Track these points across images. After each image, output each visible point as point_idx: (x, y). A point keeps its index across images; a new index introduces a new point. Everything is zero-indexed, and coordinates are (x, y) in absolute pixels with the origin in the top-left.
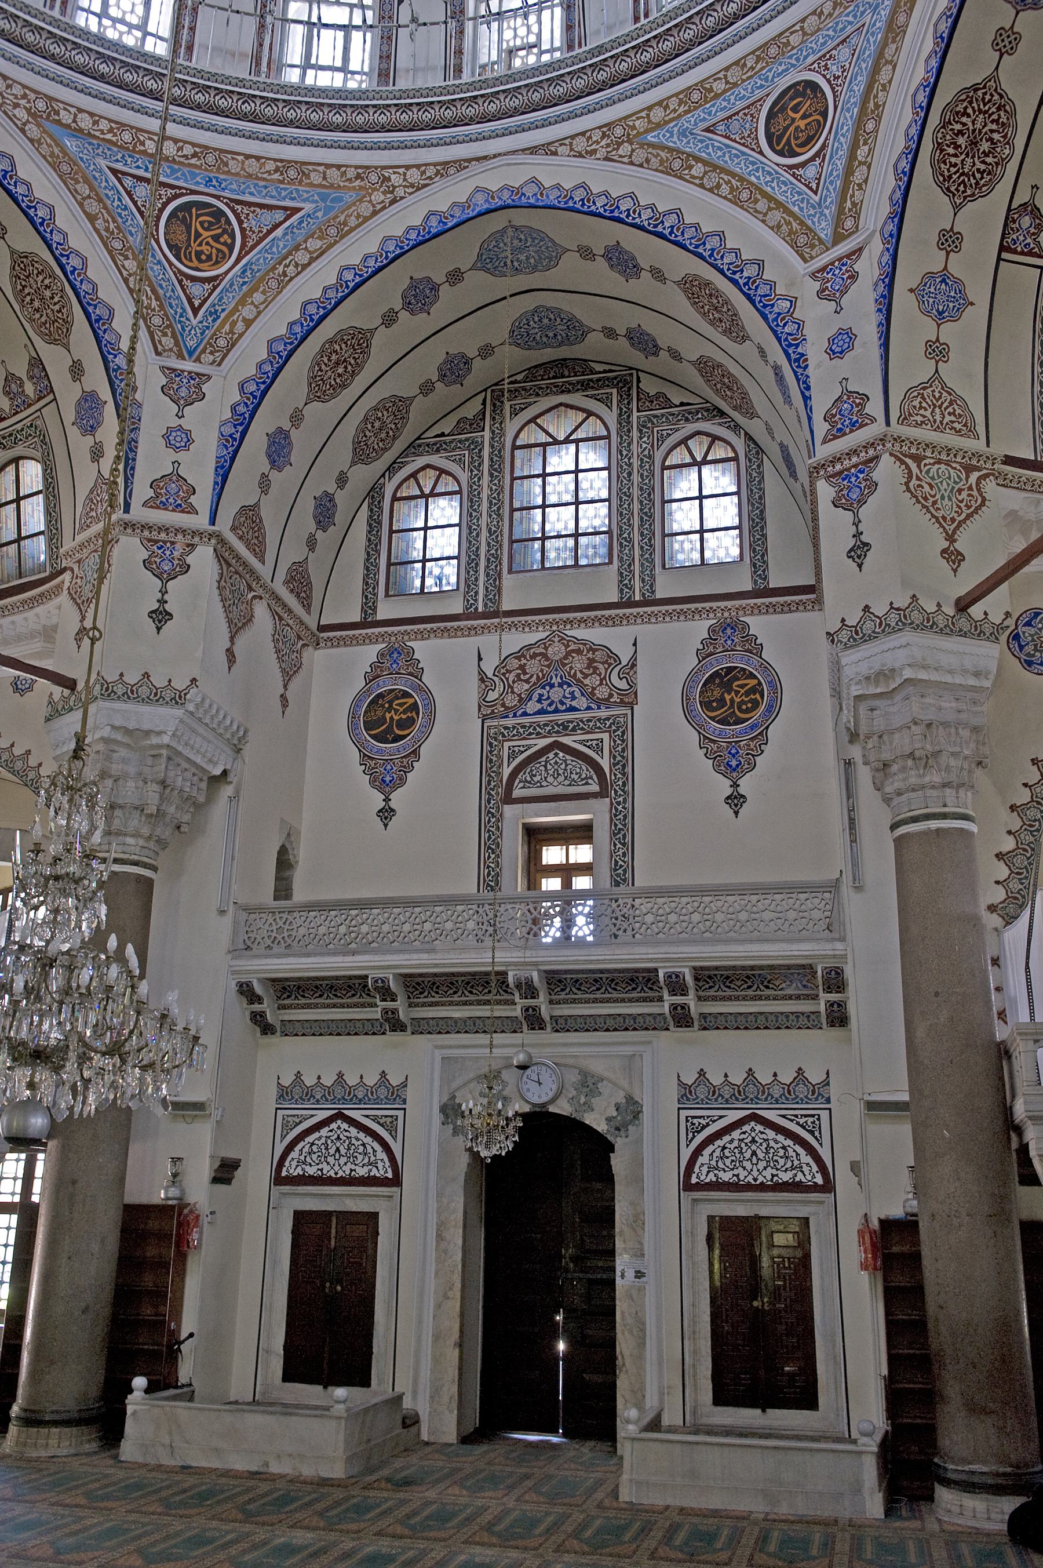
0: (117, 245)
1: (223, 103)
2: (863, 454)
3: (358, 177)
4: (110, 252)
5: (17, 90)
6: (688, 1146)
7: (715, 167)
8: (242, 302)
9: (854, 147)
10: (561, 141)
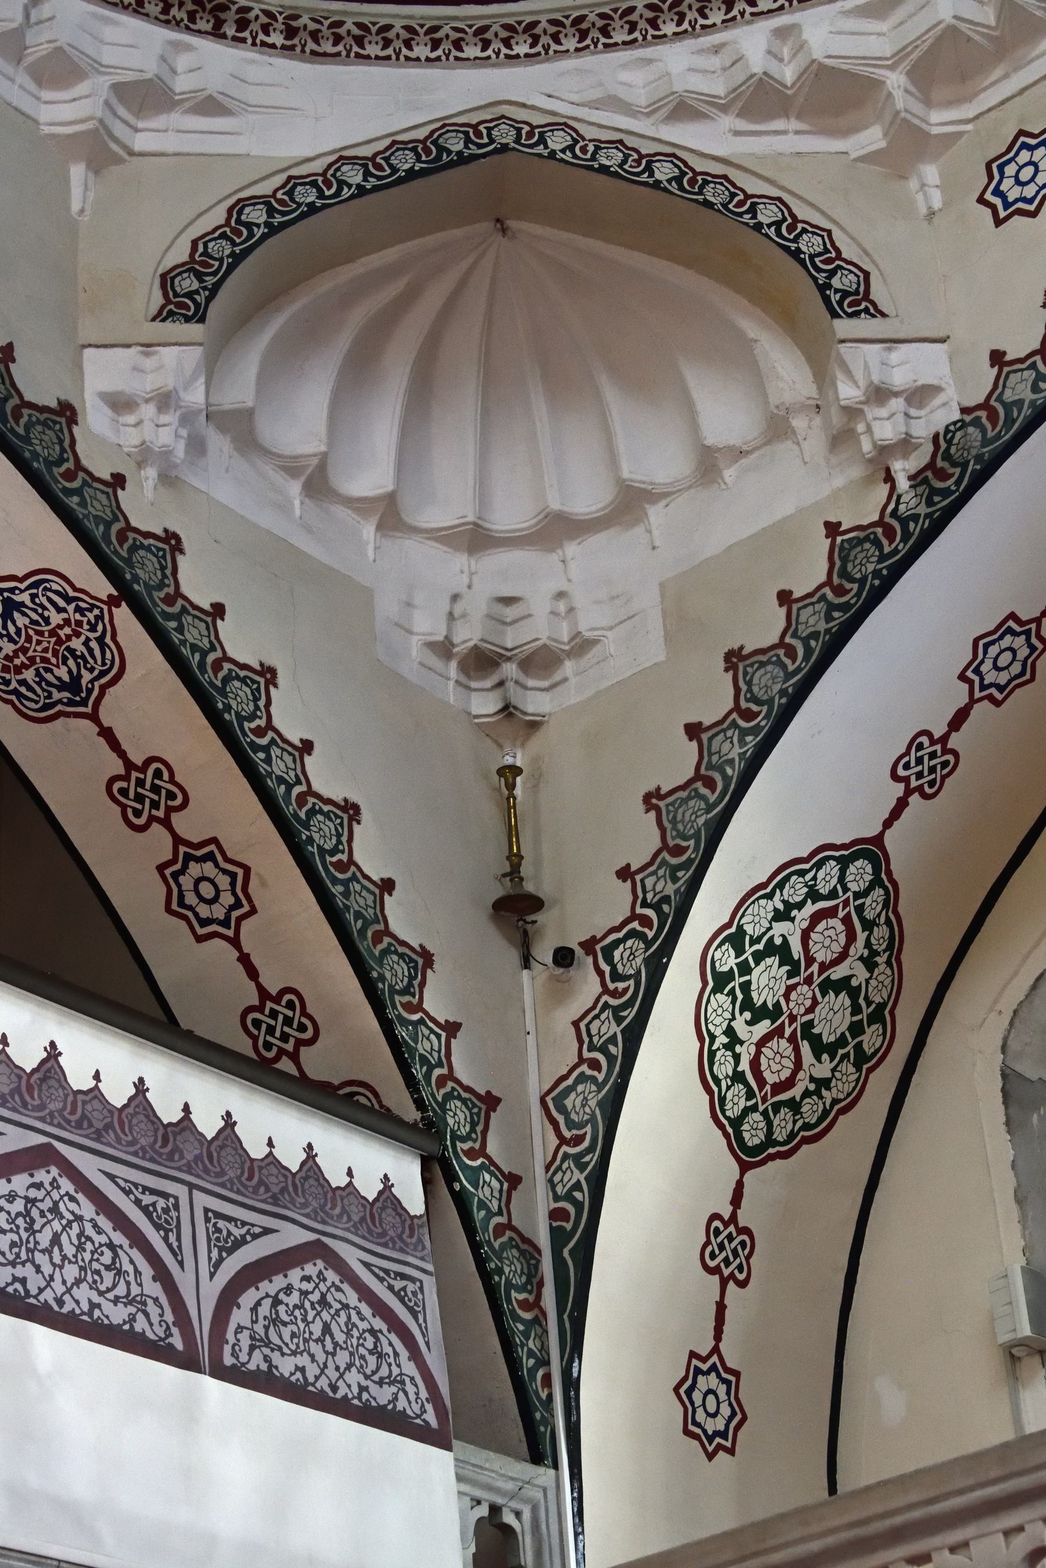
6: (212, 1275)
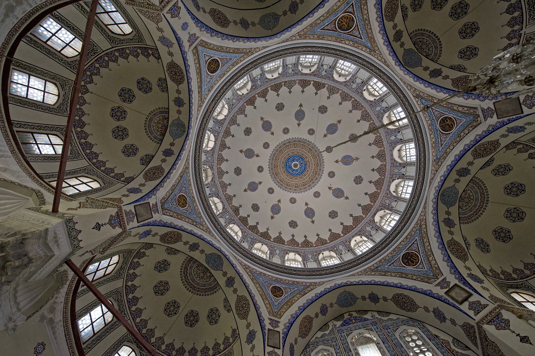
0: (367, 22)
1: (333, 51)
2: (165, 3)
3: (306, 37)
4: (369, 20)
5: (376, 56)
7: (228, 52)
8: (339, 6)
9: (200, 66)
10: (262, 49)
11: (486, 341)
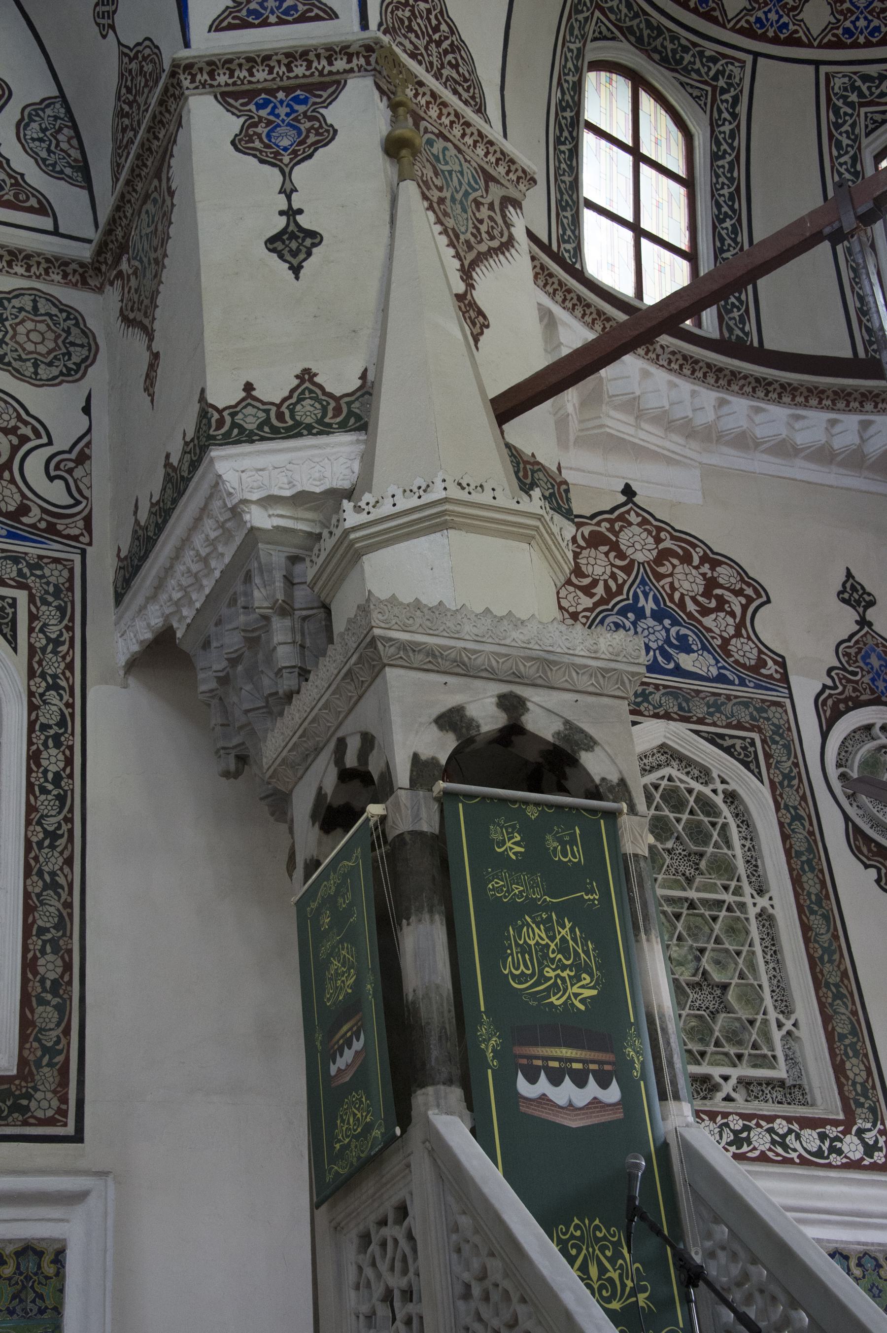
11: (158, 175)
